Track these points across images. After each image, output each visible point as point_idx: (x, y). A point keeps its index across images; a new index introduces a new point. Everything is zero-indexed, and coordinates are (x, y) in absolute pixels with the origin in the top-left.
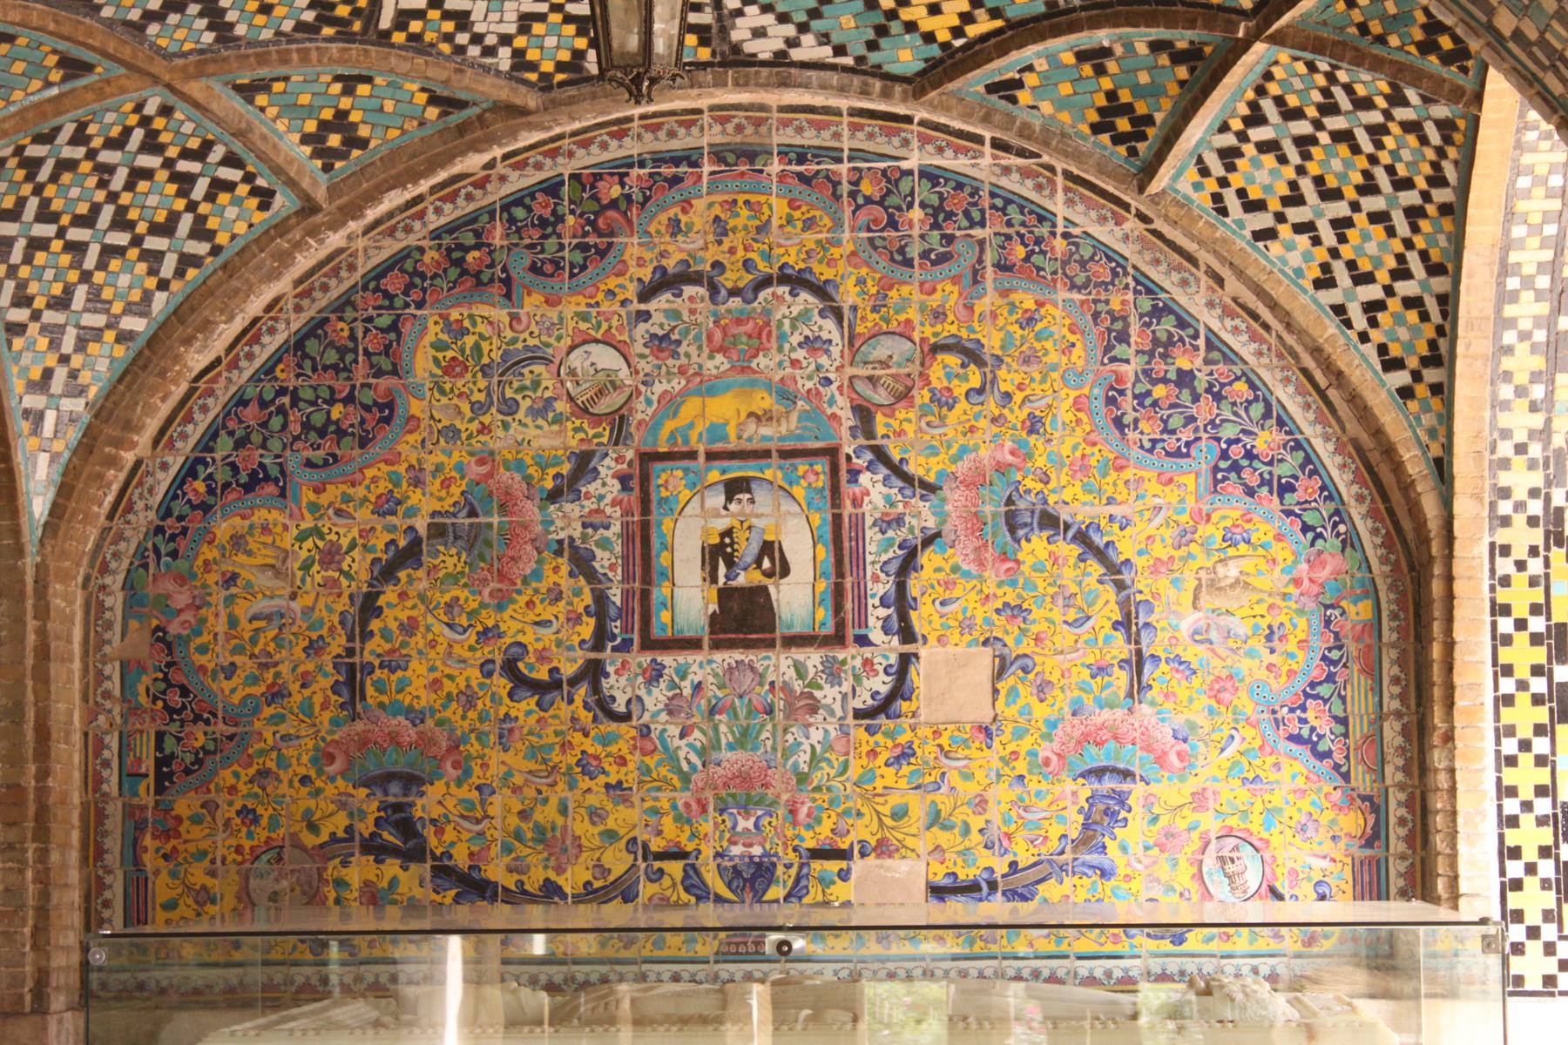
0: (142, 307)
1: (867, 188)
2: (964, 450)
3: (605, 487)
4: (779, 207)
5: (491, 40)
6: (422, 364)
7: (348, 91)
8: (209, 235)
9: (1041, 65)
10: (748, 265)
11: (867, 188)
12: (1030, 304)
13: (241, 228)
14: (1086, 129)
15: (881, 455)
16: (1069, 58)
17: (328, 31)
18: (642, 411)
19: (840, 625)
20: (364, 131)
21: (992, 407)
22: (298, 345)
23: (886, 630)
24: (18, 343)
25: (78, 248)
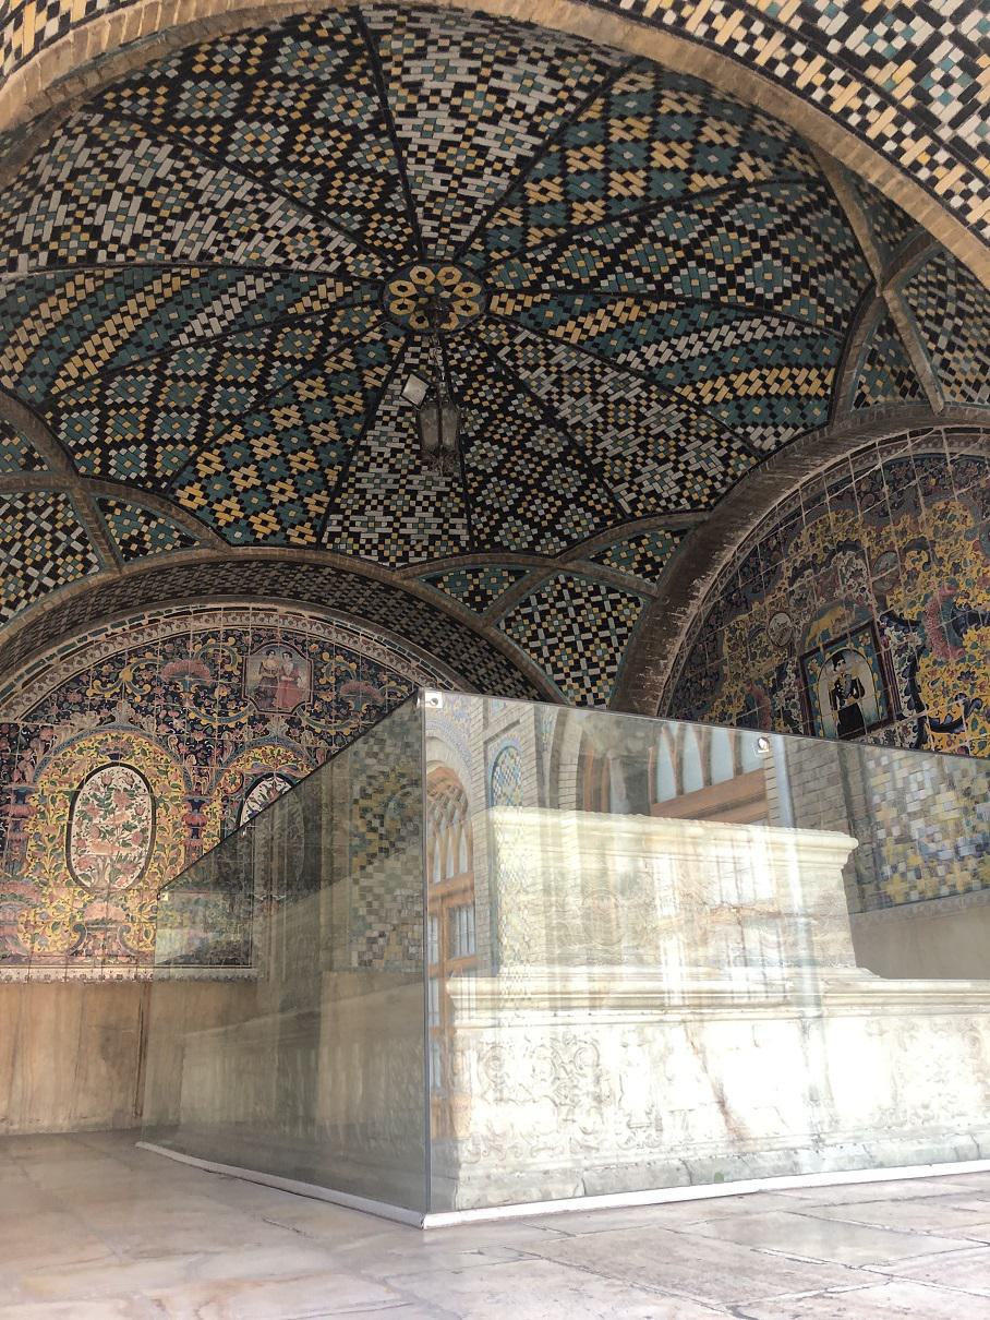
0: (612, 662)
1: (864, 488)
2: (927, 597)
3: (791, 678)
4: (832, 515)
5: (674, 498)
6: (725, 650)
7: (639, 545)
8: (623, 624)
9: (863, 379)
10: (825, 549)
11: (864, 488)
12: (942, 506)
13: (635, 617)
14: (900, 398)
15: (891, 615)
16: (867, 367)
17: (610, 523)
18: (798, 637)
19: (890, 712)
20: (658, 559)
21: (936, 569)
22: (689, 659)
23: (910, 708)
24: (565, 688)
25: (572, 645)
